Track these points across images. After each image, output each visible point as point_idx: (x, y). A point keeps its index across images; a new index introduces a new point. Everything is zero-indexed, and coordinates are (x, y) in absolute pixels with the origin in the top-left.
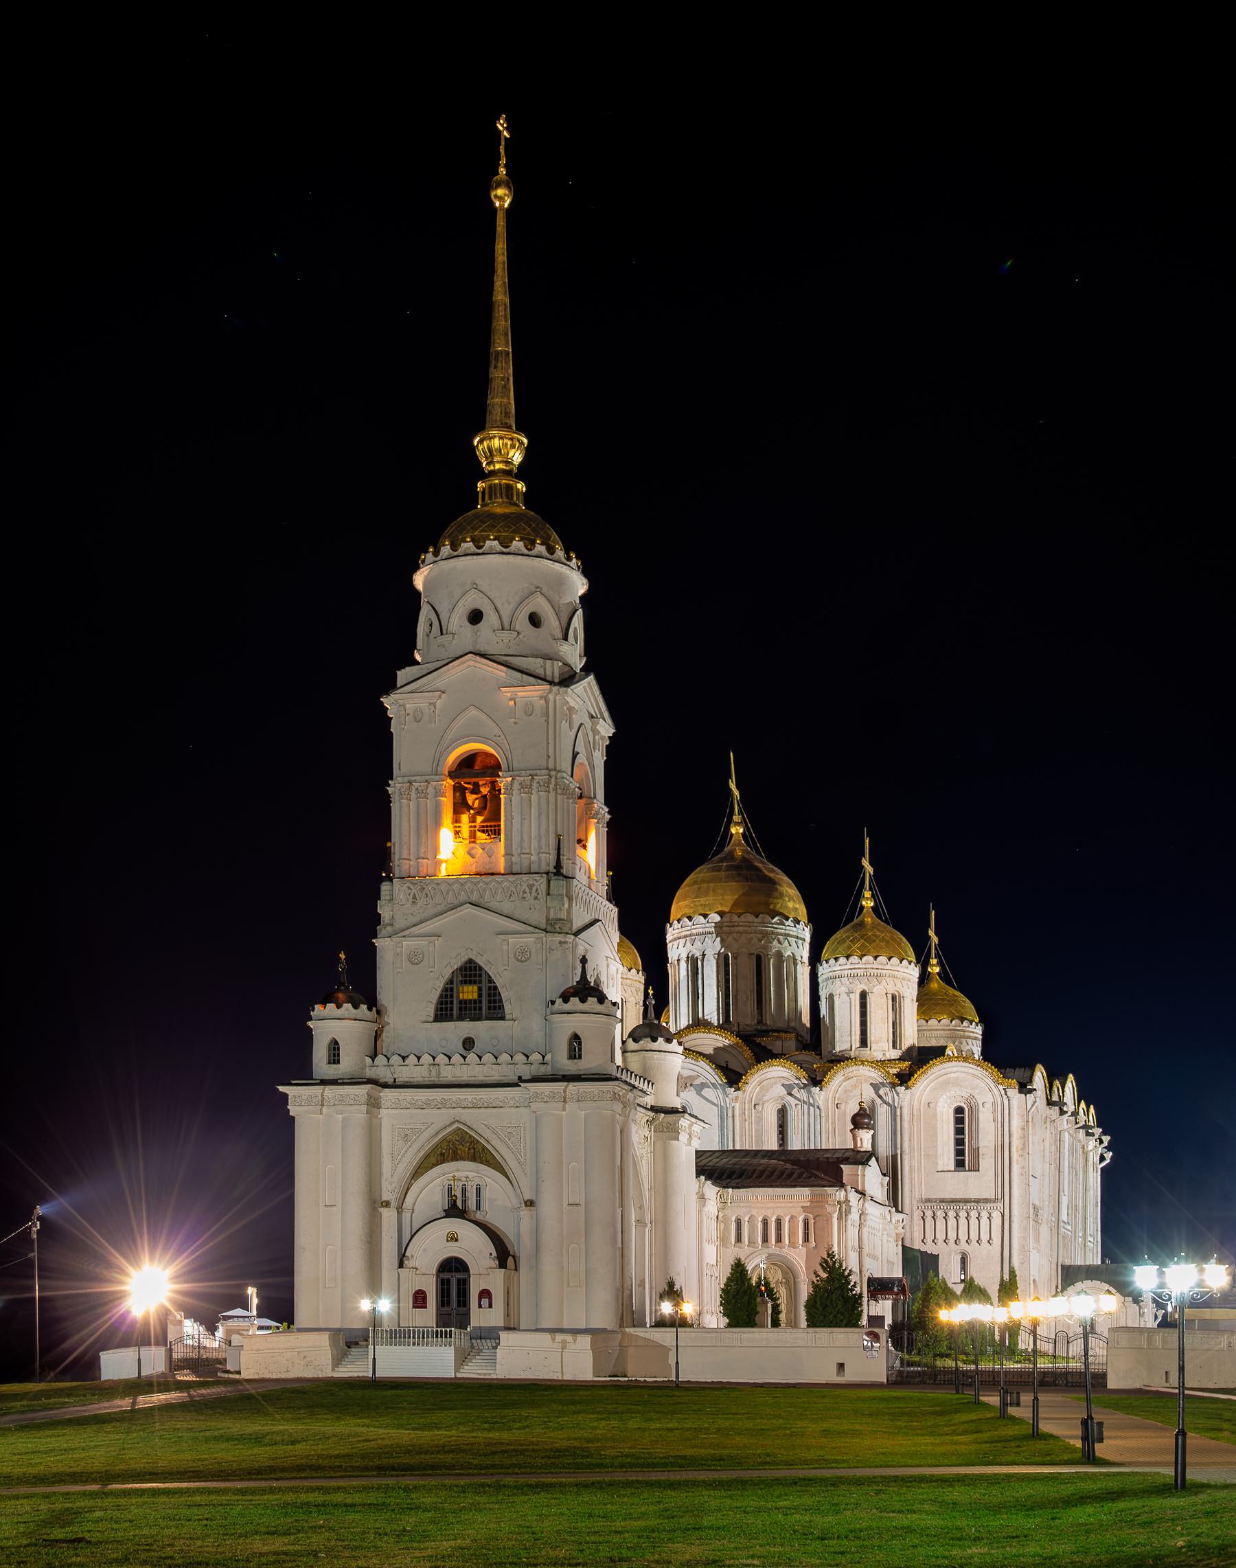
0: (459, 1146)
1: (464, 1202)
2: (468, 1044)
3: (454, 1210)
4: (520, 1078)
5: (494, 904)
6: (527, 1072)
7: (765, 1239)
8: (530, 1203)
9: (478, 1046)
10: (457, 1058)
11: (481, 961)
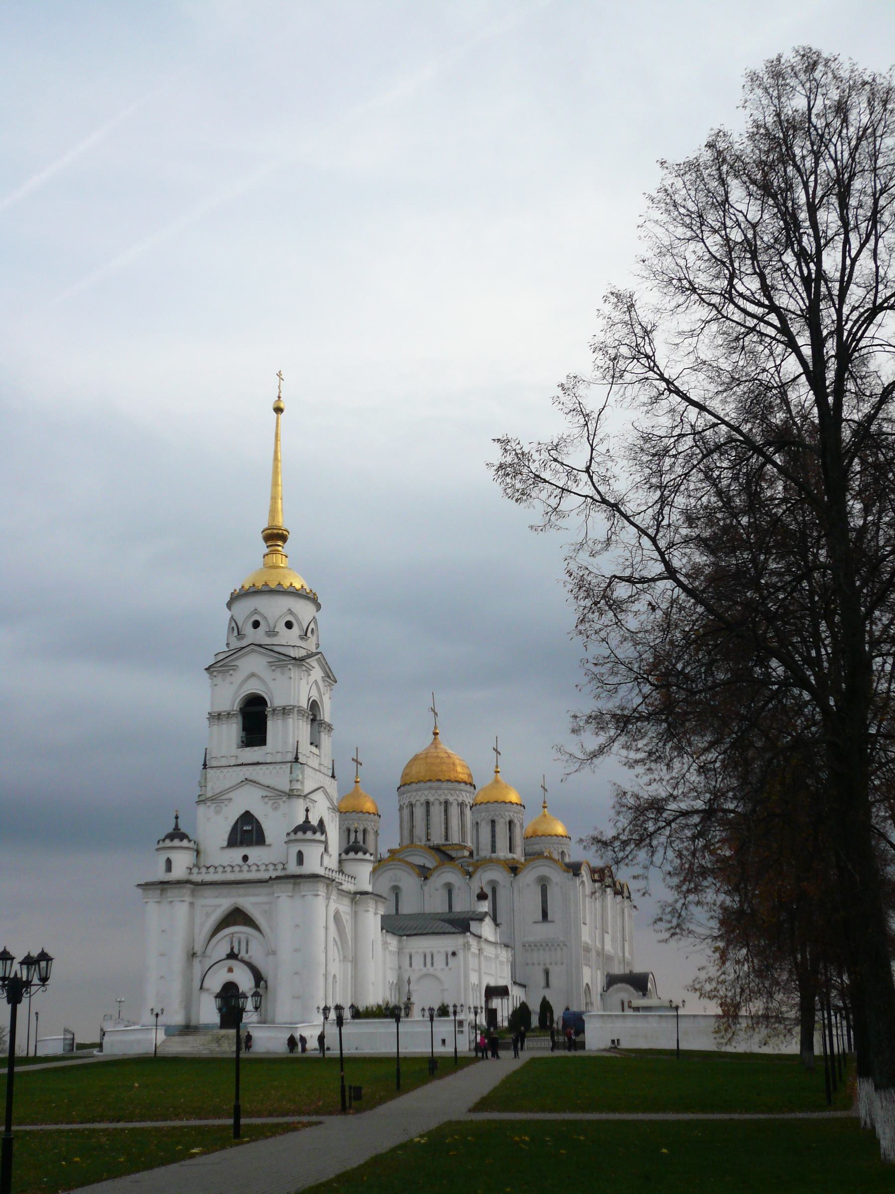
1: (239, 950)
2: (245, 858)
3: (232, 956)
5: (261, 782)
7: (425, 965)
9: (250, 862)
10: (237, 869)
11: (252, 812)
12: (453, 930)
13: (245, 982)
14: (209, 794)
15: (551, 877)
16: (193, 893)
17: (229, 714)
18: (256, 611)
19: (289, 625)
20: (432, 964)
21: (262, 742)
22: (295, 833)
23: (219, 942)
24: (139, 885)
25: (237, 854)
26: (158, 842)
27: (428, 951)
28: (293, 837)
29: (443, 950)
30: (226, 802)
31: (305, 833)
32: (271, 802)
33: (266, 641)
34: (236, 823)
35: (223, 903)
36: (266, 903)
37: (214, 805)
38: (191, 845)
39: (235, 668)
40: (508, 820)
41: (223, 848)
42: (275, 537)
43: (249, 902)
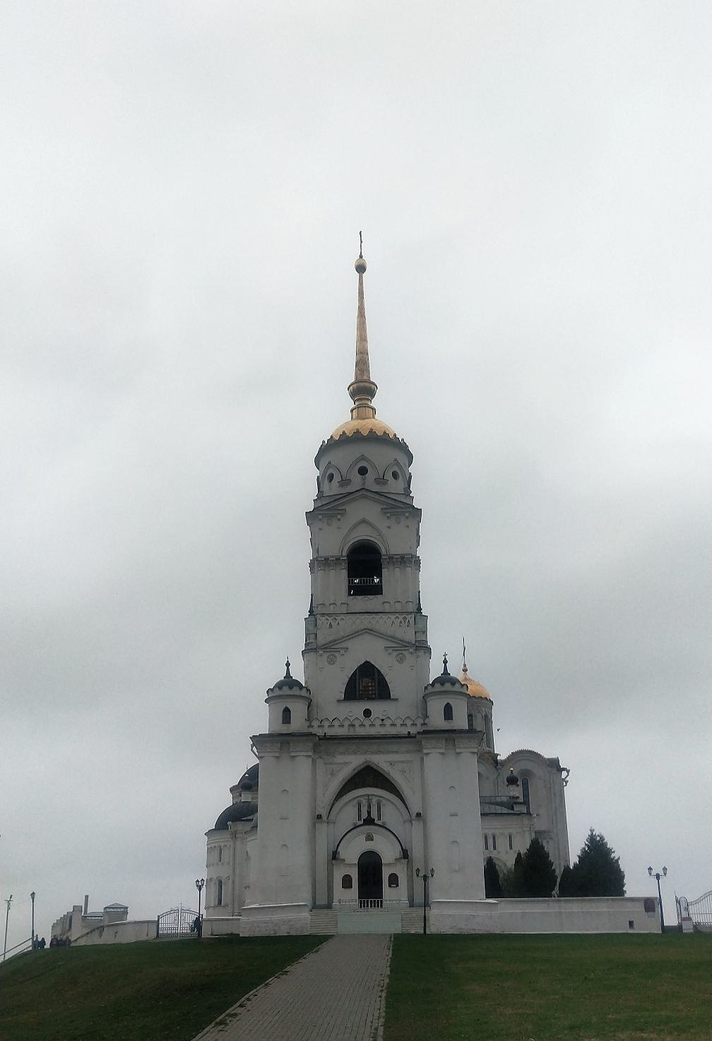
0: (369, 776)
2: (367, 713)
3: (369, 821)
4: (409, 732)
6: (413, 731)
7: (487, 848)
8: (419, 815)
12: (505, 811)
13: (387, 851)
14: (321, 640)
15: (535, 771)
16: (315, 749)
17: (338, 559)
18: (363, 458)
19: (395, 475)
20: (495, 848)
21: (377, 590)
22: (442, 684)
23: (346, 804)
24: (253, 738)
25: (357, 708)
26: (267, 692)
27: (490, 833)
28: (438, 687)
29: (507, 832)
30: (342, 651)
31: (442, 684)
32: (395, 653)
33: (376, 488)
34: (354, 674)
35: (351, 762)
36: (402, 762)
37: (326, 655)
38: (307, 695)
39: (343, 513)
40: (483, 714)
41: (339, 701)
42: (363, 391)
43: (382, 761)
